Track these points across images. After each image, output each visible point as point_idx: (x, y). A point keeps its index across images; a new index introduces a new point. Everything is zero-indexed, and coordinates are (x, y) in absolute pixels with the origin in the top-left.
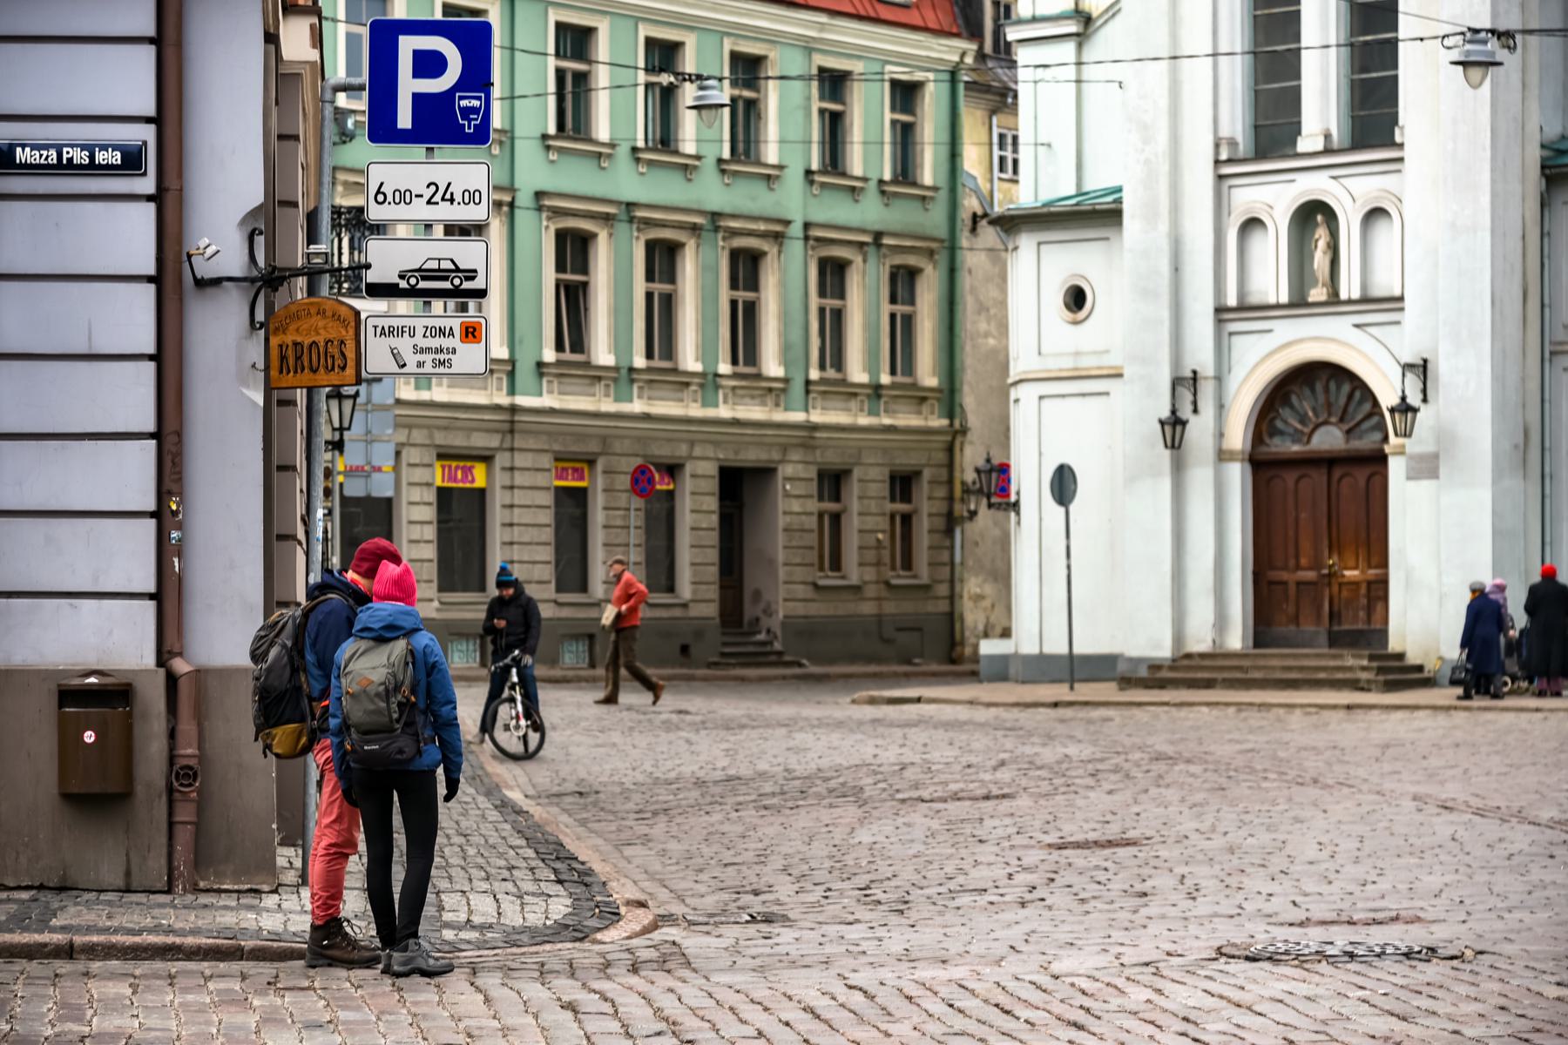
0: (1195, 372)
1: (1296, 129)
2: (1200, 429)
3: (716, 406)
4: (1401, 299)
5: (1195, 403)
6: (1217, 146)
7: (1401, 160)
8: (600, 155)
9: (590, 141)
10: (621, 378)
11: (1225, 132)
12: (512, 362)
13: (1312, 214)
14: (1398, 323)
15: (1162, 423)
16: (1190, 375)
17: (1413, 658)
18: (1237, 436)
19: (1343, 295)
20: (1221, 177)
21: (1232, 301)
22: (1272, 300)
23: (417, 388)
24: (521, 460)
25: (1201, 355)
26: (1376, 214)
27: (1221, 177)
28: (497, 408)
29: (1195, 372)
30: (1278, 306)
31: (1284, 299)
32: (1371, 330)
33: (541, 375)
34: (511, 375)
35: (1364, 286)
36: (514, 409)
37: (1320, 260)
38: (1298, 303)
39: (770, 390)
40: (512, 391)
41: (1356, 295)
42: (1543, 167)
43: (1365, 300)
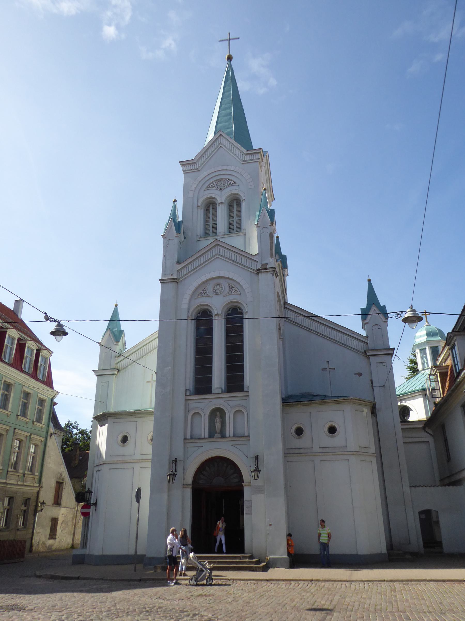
0: (176, 459)
5: (176, 469)
7: (249, 396)
11: (188, 388)
16: (175, 460)
18: (189, 479)
19: (228, 435)
20: (186, 400)
21: (189, 437)
22: (203, 436)
25: (179, 453)
27: (186, 400)
30: (205, 438)
32: (238, 446)
37: (218, 425)
41: (229, 436)
43: (235, 436)
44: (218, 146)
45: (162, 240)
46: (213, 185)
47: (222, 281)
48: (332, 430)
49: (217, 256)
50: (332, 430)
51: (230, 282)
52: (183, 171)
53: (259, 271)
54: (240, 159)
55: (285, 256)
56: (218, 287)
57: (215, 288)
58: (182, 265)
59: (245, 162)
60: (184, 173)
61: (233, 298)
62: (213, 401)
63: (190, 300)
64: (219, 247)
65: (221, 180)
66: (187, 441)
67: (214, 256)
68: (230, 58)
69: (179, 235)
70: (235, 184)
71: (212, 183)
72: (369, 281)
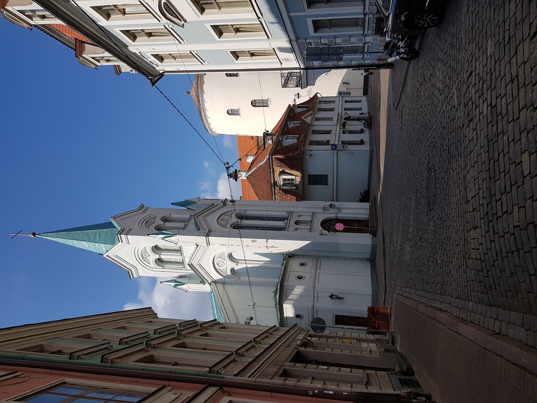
44: (116, 257)
46: (146, 260)
65: (142, 256)
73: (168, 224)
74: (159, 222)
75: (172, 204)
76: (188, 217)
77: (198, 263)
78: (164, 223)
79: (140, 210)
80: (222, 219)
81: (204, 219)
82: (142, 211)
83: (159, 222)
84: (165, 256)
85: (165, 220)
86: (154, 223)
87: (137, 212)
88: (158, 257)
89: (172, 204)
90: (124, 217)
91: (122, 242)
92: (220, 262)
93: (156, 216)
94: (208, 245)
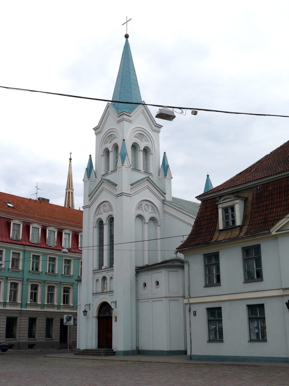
0: (90, 303)
1: (103, 265)
2: (90, 313)
3: (60, 310)
4: (113, 291)
6: (93, 268)
7: (113, 269)
8: (40, 273)
9: (55, 273)
10: (43, 306)
12: (22, 304)
13: (104, 278)
14: (113, 295)
15: (83, 312)
17: (115, 350)
18: (95, 314)
22: (99, 292)
23: (3, 307)
24: (22, 318)
26: (111, 278)
28: (18, 310)
29: (90, 303)
30: (100, 293)
31: (101, 292)
33: (27, 305)
34: (21, 305)
35: (110, 289)
36: (21, 310)
38: (102, 293)
39: (70, 307)
40: (21, 308)
41: (109, 291)
42: (136, 270)
44: (108, 113)
45: (83, 182)
46: (107, 139)
47: (106, 204)
48: (158, 283)
49: (103, 189)
50: (158, 283)
51: (109, 203)
52: (95, 134)
53: (118, 196)
54: (116, 120)
55: (168, 166)
56: (105, 207)
57: (104, 208)
58: (91, 196)
59: (119, 122)
60: (96, 135)
61: (110, 213)
62: (103, 273)
63: (94, 216)
64: (104, 183)
66: (94, 295)
67: (102, 189)
68: (127, 36)
69: (89, 179)
70: (115, 138)
71: (107, 139)
72: (208, 176)
73: (141, 155)
74: (142, 145)
75: (165, 153)
76: (151, 171)
77: (105, 189)
78: (142, 150)
79: (155, 126)
80: (146, 204)
81: (146, 187)
82: (154, 128)
83: (142, 145)
84: (111, 155)
85: (146, 150)
86: (141, 140)
87: (152, 124)
88: (110, 150)
89: (165, 153)
90: (146, 112)
91: (118, 117)
92: (106, 208)
93: (149, 140)
94: (116, 195)
